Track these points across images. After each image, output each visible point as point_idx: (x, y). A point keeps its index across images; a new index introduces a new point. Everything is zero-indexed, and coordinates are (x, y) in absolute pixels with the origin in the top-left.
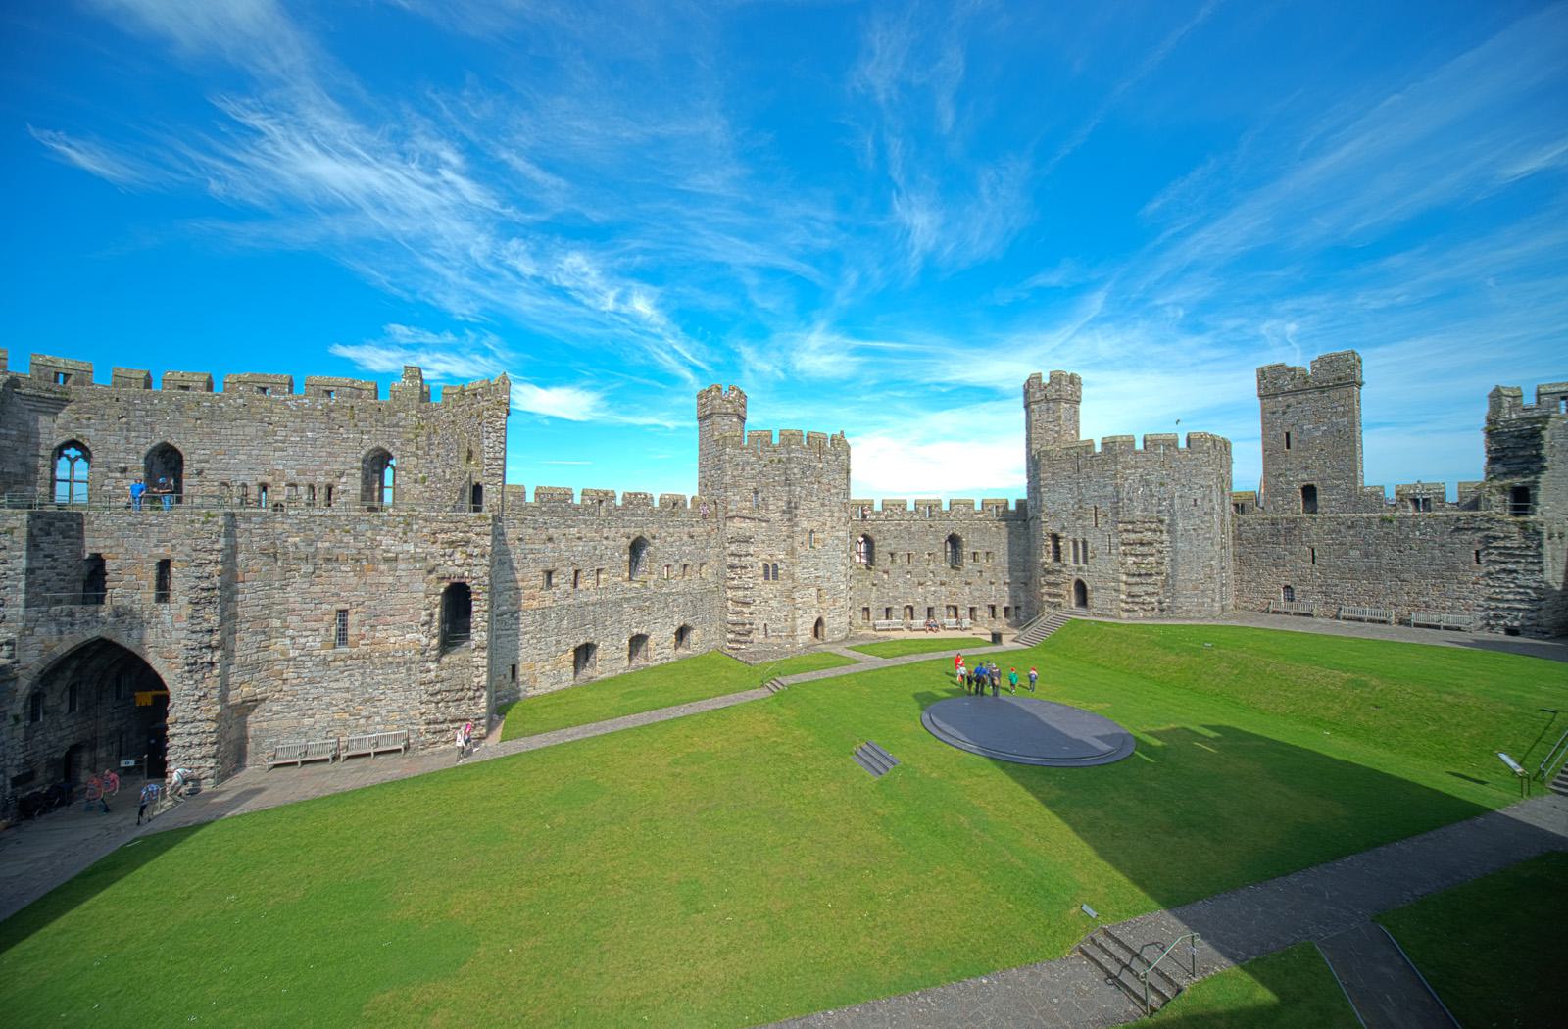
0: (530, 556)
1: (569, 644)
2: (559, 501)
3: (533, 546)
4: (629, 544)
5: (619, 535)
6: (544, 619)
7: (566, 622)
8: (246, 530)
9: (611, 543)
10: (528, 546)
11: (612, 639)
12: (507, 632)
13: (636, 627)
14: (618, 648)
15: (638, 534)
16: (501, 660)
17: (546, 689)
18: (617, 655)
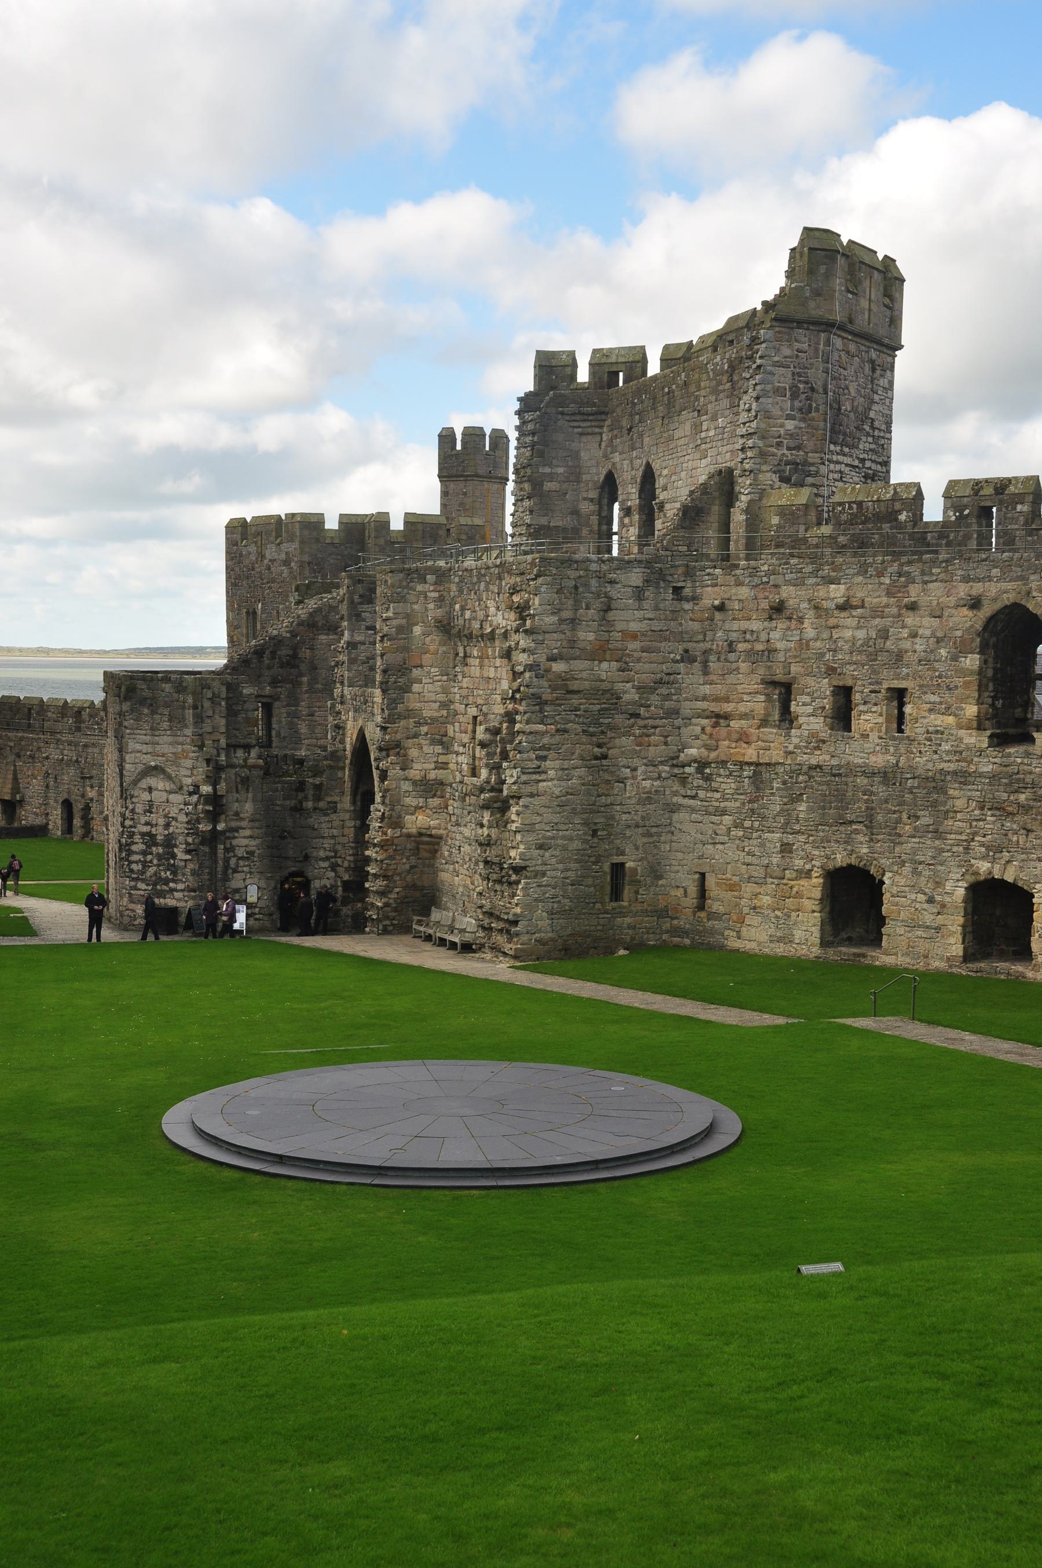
0: (741, 647)
1: (810, 858)
2: (879, 518)
3: (744, 625)
4: (979, 627)
5: (952, 600)
6: (758, 789)
7: (803, 807)
8: (421, 593)
9: (927, 621)
10: (735, 626)
11: (915, 872)
12: (691, 802)
13: (984, 858)
14: (931, 900)
15: (1009, 598)
16: (680, 855)
17: (759, 944)
18: (928, 918)
